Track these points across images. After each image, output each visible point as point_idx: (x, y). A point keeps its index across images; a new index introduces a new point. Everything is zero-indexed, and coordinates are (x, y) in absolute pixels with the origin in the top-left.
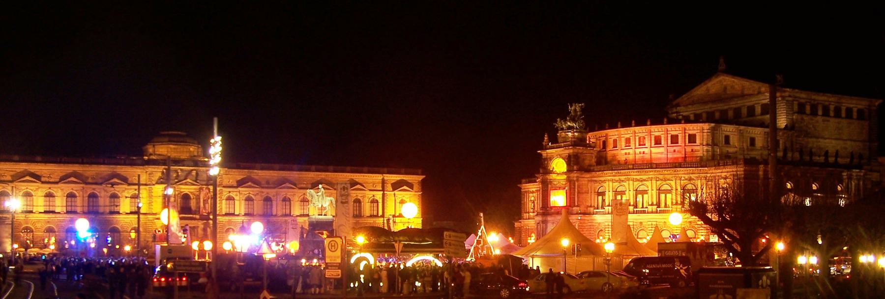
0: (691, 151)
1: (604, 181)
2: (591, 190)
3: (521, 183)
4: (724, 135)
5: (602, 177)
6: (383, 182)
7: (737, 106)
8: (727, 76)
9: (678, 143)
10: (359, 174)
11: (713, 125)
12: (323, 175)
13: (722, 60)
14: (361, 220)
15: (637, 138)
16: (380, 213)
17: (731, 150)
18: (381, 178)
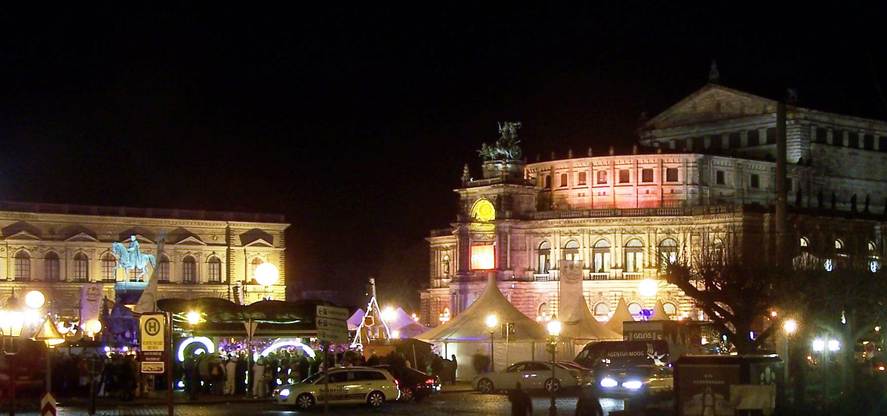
0: (670, 192)
1: (548, 234)
2: (530, 245)
3: (429, 235)
4: (716, 171)
5: (545, 227)
6: (229, 233)
7: (736, 130)
8: (721, 89)
9: (652, 181)
10: (191, 221)
11: (701, 156)
12: (136, 221)
13: (714, 66)
14: (195, 289)
15: (595, 173)
16: (224, 279)
17: (726, 192)
18: (225, 227)
